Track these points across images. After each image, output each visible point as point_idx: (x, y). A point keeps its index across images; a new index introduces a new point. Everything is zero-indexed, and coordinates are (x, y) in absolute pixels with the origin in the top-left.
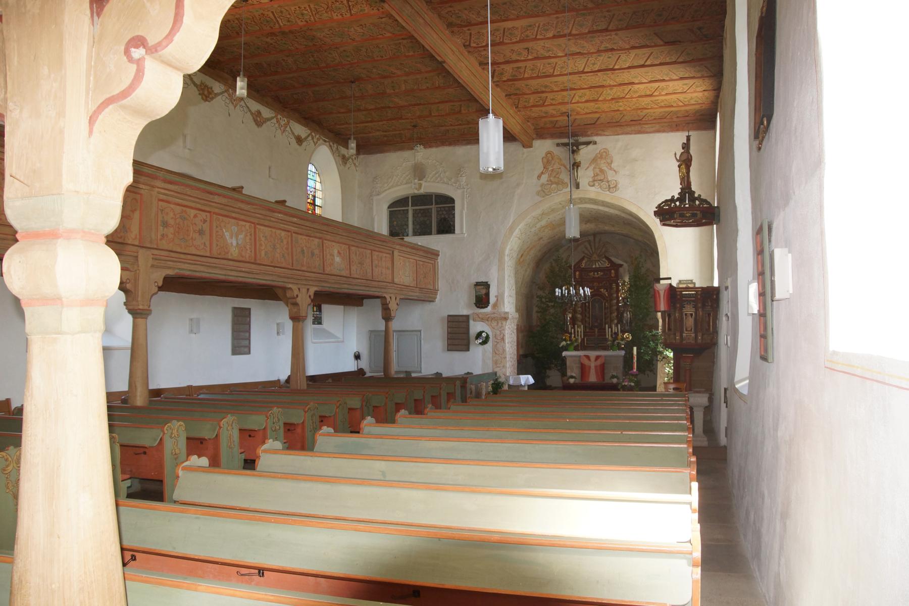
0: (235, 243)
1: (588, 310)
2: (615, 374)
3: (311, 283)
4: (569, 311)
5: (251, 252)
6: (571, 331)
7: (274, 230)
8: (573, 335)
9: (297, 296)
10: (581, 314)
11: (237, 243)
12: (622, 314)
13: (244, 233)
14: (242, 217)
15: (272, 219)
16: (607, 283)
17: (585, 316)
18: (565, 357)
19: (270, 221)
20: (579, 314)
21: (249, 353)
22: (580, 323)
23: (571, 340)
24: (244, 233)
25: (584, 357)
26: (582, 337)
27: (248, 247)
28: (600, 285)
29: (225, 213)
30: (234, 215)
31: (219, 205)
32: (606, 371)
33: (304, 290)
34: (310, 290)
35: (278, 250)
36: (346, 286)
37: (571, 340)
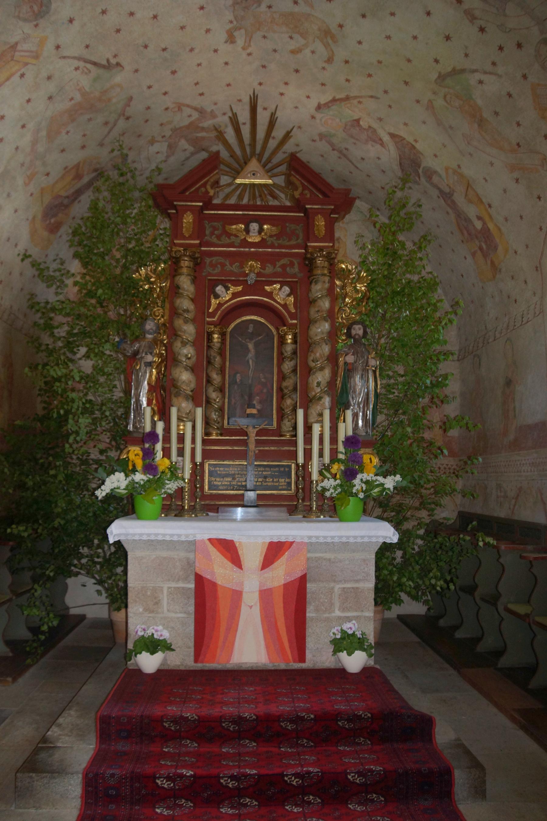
1: (218, 359)
2: (350, 627)
4: (149, 358)
6: (154, 424)
8: (159, 447)
10: (193, 369)
12: (350, 370)
16: (292, 264)
17: (209, 381)
18: (118, 544)
20: (186, 368)
22: (186, 405)
23: (150, 468)
25: (213, 551)
26: (199, 459)
28: (269, 269)
32: (310, 613)
37: (150, 468)
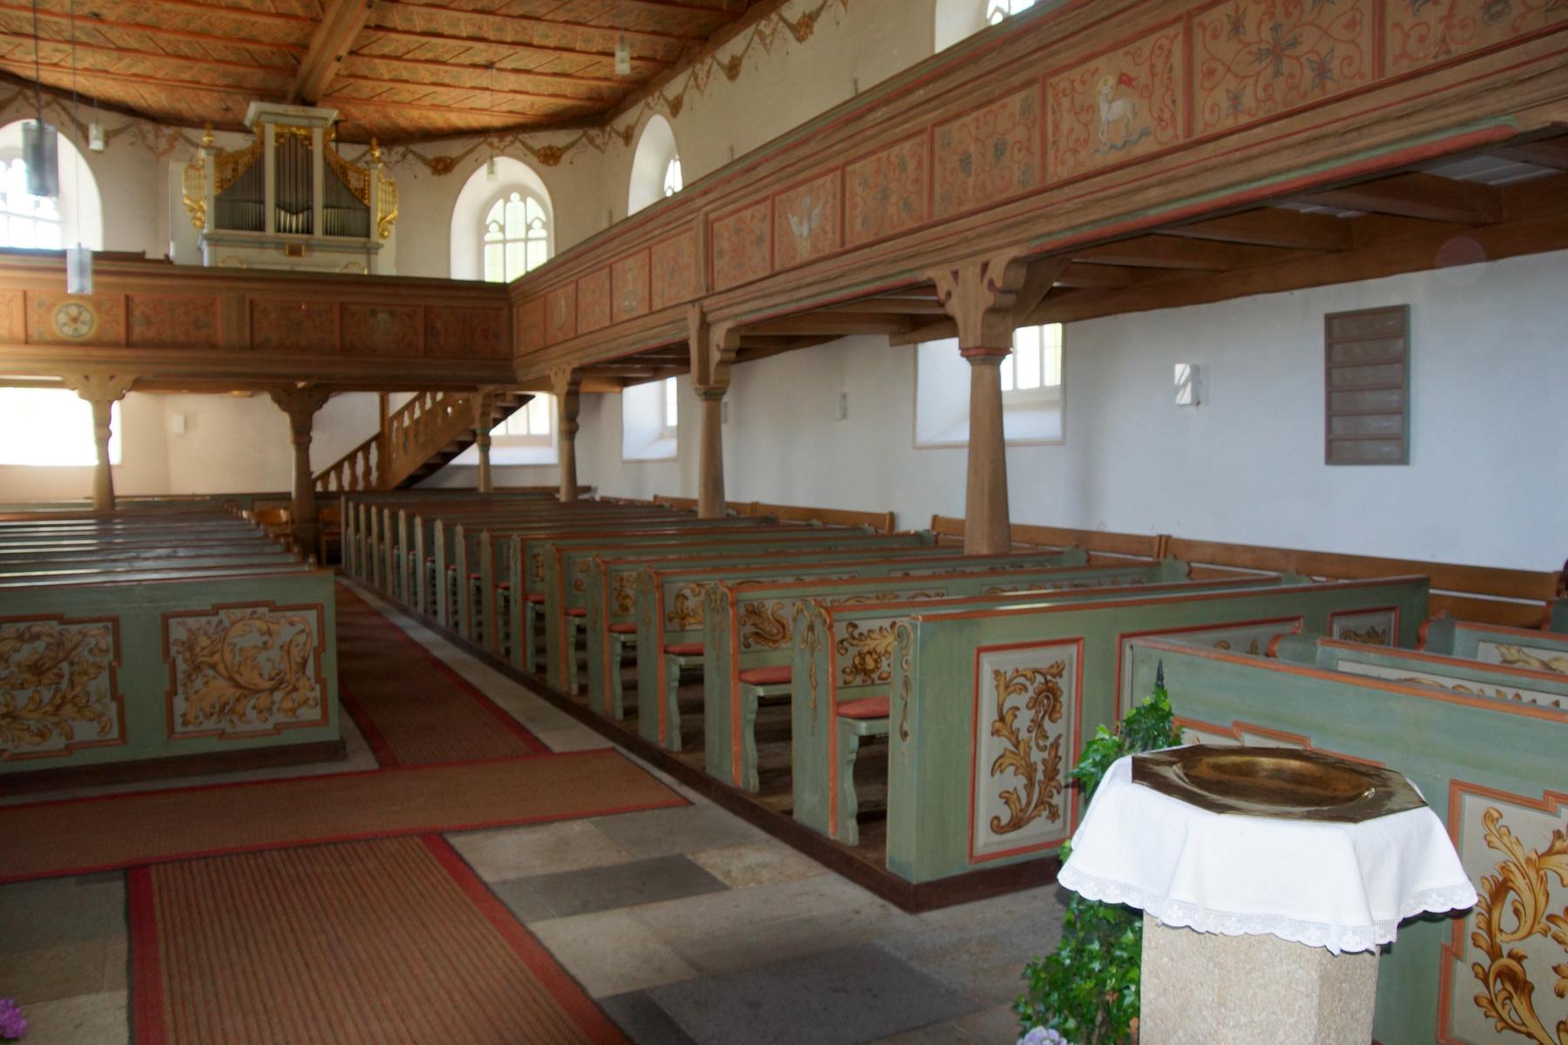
0: (805, 233)
3: (986, 243)
5: (834, 233)
7: (883, 155)
9: (949, 294)
11: (810, 229)
13: (821, 202)
14: (816, 170)
15: (868, 133)
19: (866, 140)
21: (1403, 458)
24: (821, 202)
27: (828, 227)
29: (786, 184)
30: (801, 177)
31: (773, 178)
33: (970, 272)
34: (991, 266)
35: (893, 199)
36: (1154, 194)
